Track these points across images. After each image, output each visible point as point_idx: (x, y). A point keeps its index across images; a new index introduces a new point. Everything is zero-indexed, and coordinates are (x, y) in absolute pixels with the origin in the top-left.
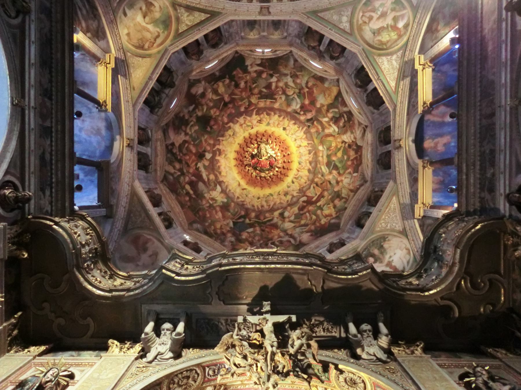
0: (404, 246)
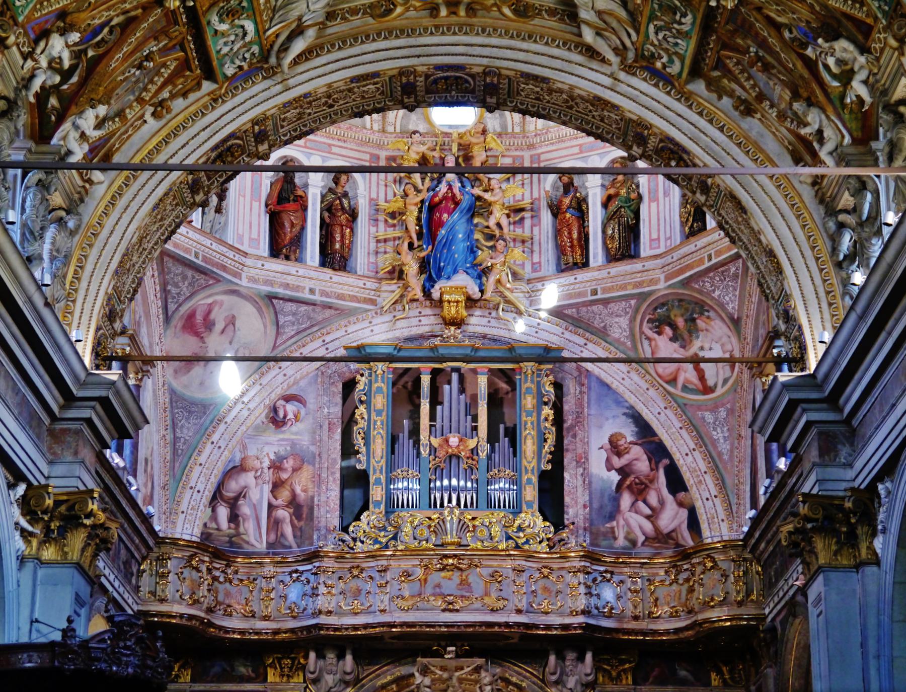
0: (729, 347)
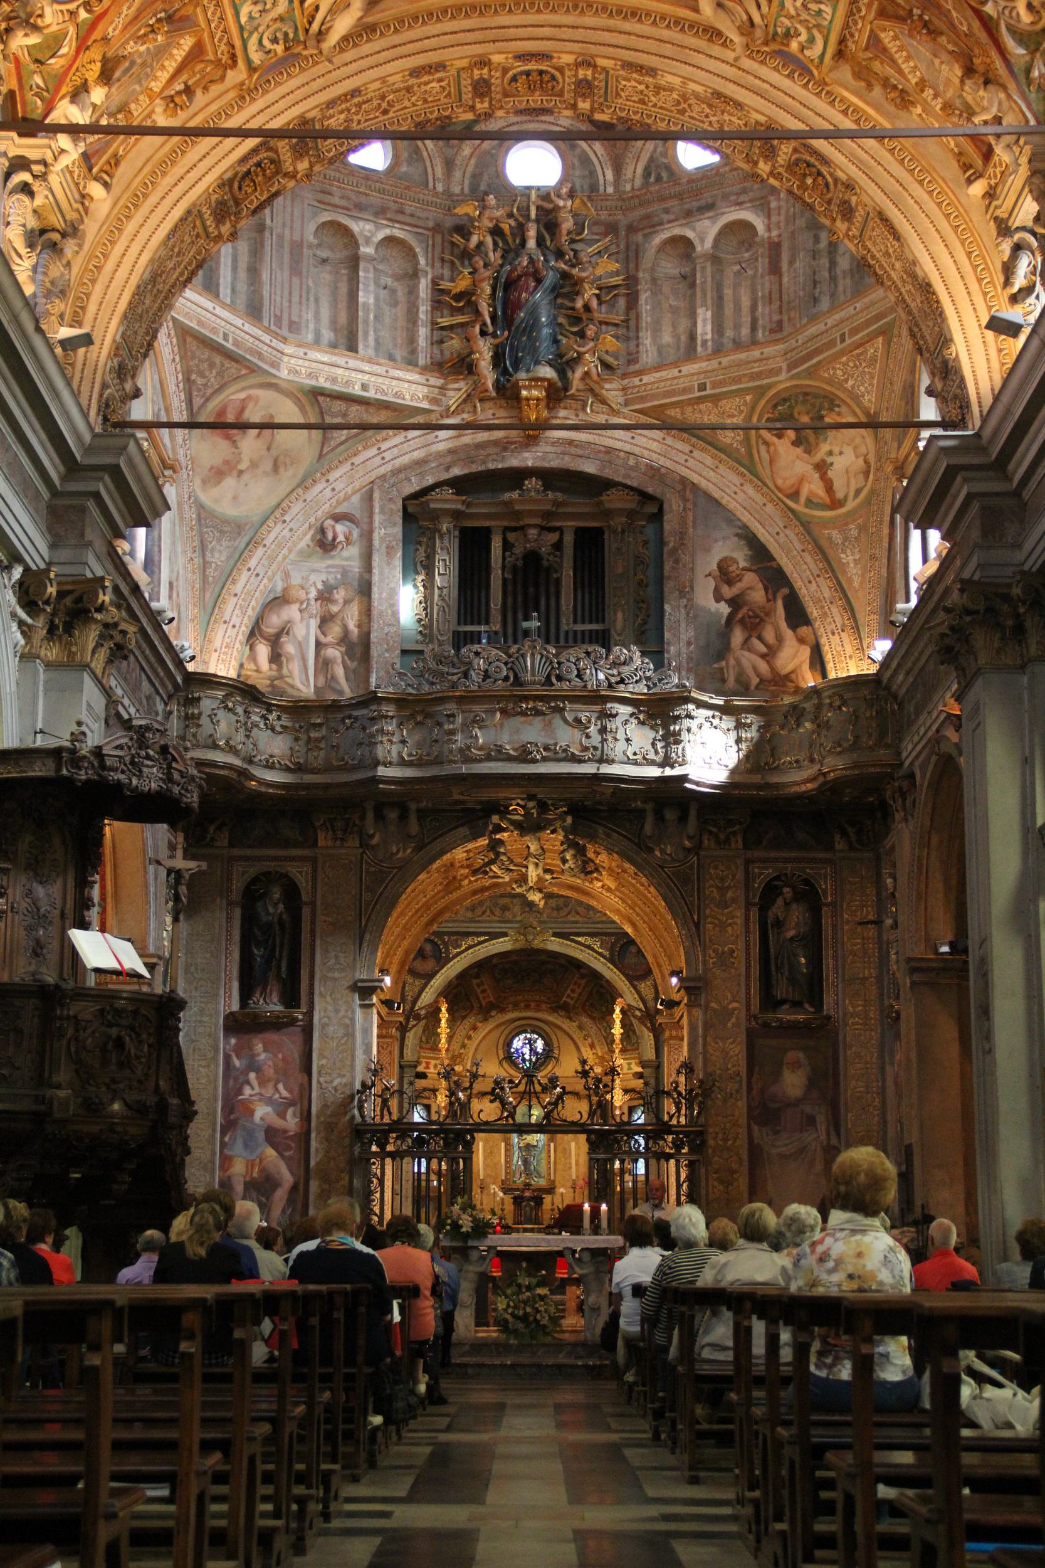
0: (863, 450)
